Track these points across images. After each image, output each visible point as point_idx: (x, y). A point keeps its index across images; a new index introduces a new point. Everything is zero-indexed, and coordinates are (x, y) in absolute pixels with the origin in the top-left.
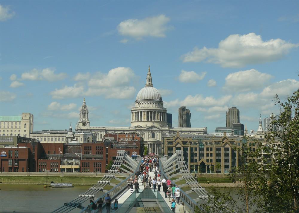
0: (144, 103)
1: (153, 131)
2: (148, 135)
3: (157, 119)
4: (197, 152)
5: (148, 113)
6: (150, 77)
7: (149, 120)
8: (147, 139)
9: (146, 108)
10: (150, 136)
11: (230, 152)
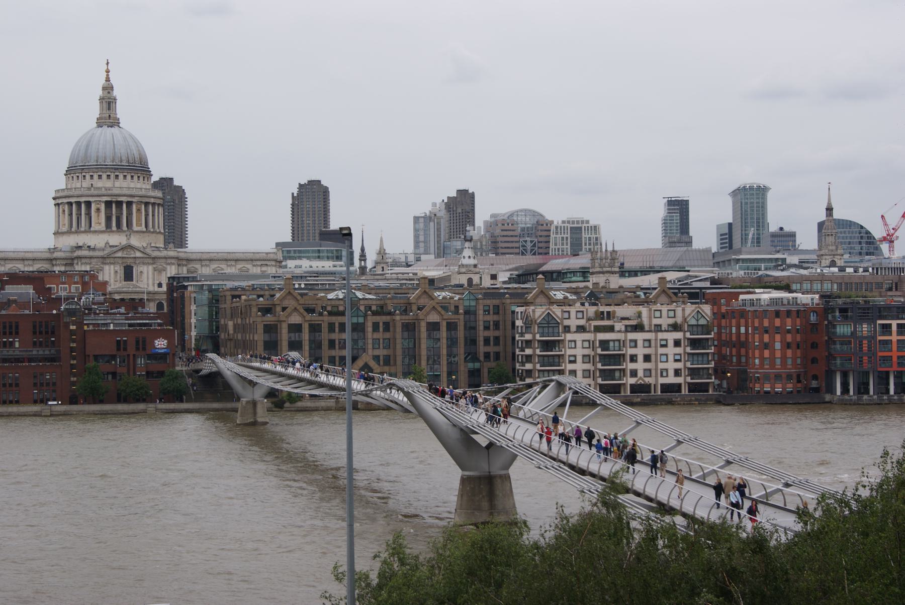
0: (96, 176)
1: (129, 262)
2: (112, 272)
3: (139, 224)
4: (347, 336)
5: (108, 204)
7: (114, 228)
9: (103, 192)
11: (443, 333)
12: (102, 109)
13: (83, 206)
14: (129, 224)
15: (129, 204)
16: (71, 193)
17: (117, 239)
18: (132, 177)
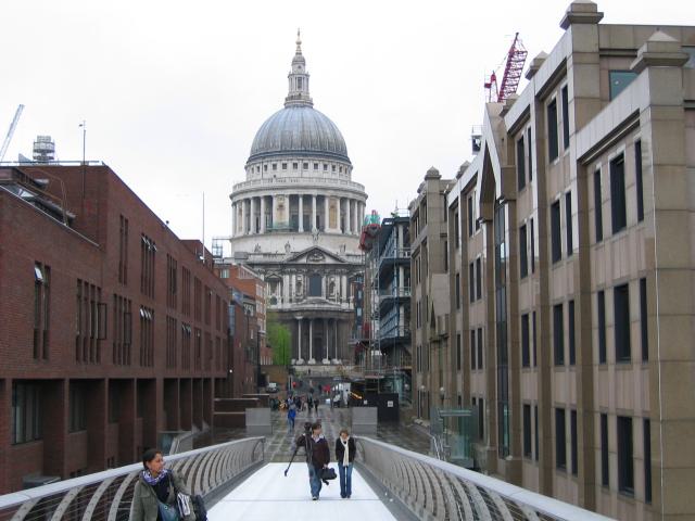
0: (279, 166)
2: (294, 284)
3: (333, 225)
5: (294, 199)
6: (299, 71)
7: (301, 229)
8: (291, 301)
9: (288, 183)
12: (291, 85)
13: (262, 202)
14: (320, 226)
15: (320, 199)
16: (248, 187)
18: (325, 166)
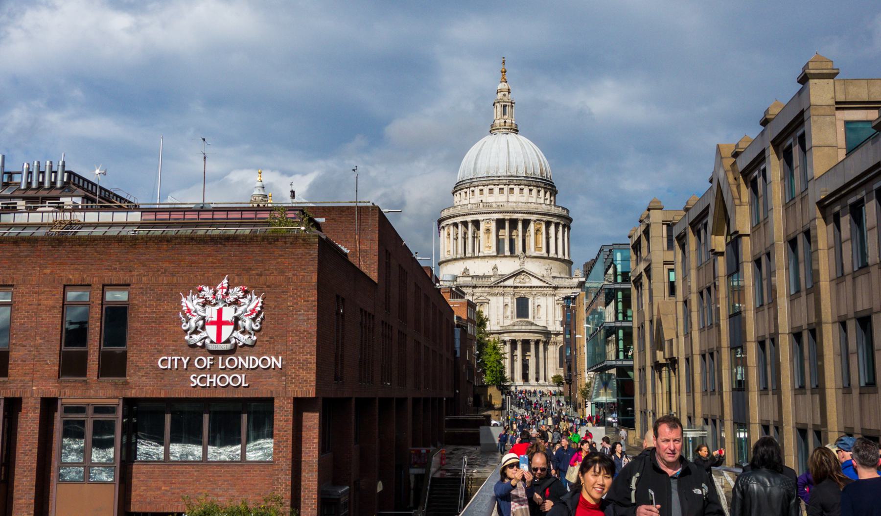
1: (522, 292)
2: (501, 306)
3: (537, 248)
5: (500, 224)
6: (505, 99)
7: (507, 253)
8: (498, 323)
10: (509, 309)
13: (470, 225)
17: (507, 266)
18: (531, 190)
